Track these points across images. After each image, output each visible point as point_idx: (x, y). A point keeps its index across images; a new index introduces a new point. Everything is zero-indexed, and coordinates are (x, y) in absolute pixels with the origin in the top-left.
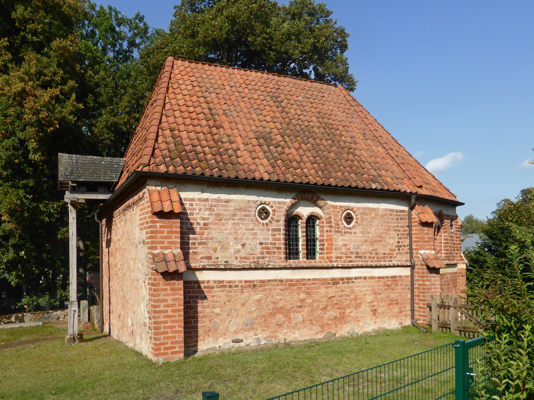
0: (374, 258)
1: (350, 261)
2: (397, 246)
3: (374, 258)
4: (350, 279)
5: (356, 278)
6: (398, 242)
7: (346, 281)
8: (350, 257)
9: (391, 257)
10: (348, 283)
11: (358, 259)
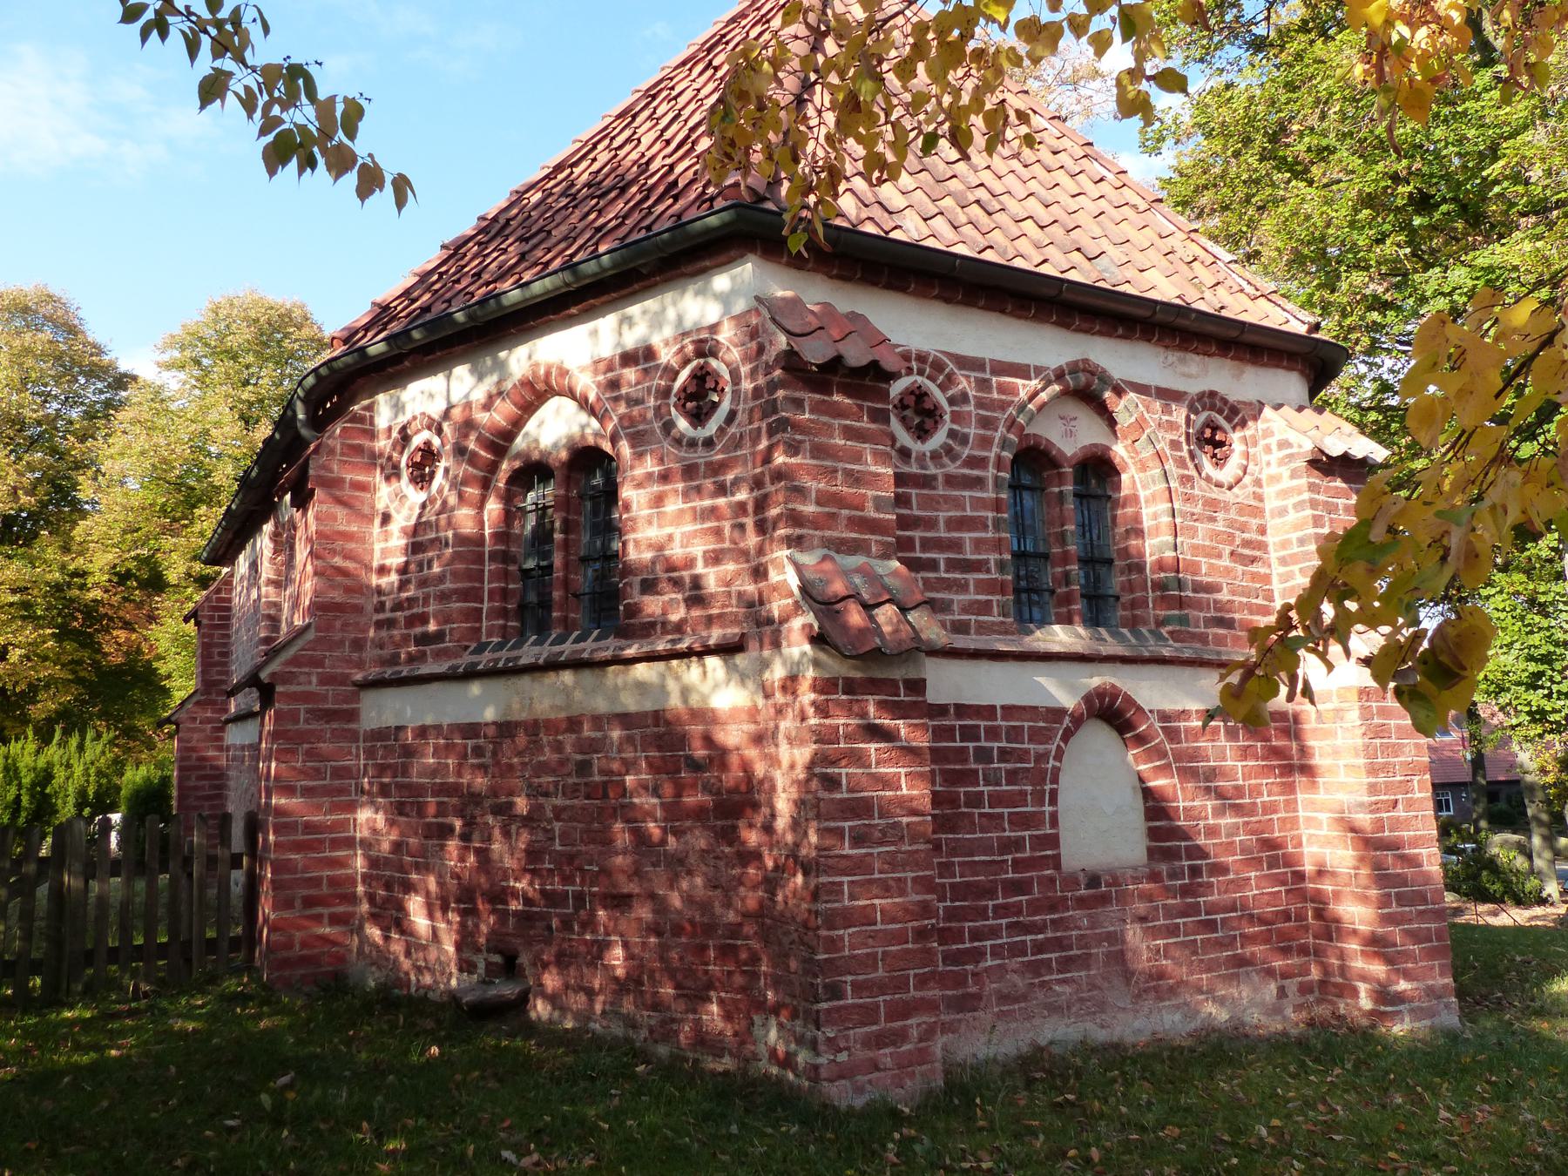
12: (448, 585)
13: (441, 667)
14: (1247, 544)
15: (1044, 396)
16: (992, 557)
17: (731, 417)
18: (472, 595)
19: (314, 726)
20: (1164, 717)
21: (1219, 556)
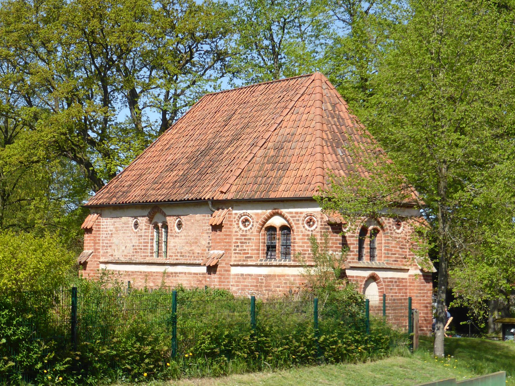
0: (191, 257)
1: (177, 259)
2: (207, 247)
3: (191, 257)
4: (176, 273)
5: (180, 273)
6: (209, 243)
7: (174, 275)
8: (177, 256)
9: (203, 256)
10: (175, 276)
11: (182, 258)
12: (254, 248)
13: (254, 263)
14: (402, 245)
15: (366, 220)
16: (355, 250)
17: (316, 227)
18: (258, 250)
19: (225, 273)
20: (383, 278)
21: (396, 248)
